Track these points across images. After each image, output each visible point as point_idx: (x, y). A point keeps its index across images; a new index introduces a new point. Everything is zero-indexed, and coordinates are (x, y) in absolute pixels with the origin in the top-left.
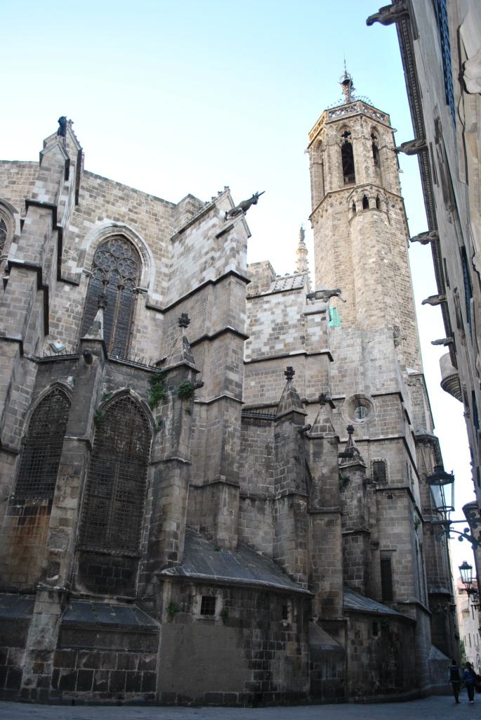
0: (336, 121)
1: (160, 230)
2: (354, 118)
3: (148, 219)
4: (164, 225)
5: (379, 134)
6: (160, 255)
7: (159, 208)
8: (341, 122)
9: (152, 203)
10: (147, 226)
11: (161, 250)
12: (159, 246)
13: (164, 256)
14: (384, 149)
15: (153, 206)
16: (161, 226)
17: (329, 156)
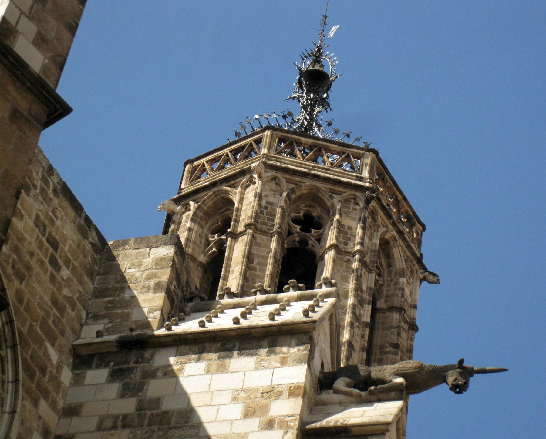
0: (294, 172)
1: (55, 302)
2: (348, 193)
3: (34, 247)
4: (66, 292)
5: (389, 266)
6: (38, 386)
7: (67, 230)
8: (308, 182)
9: (56, 201)
10: (29, 268)
11: (43, 370)
12: (41, 354)
13: (45, 394)
14: (396, 316)
15: (54, 212)
16: (60, 288)
17: (249, 258)
